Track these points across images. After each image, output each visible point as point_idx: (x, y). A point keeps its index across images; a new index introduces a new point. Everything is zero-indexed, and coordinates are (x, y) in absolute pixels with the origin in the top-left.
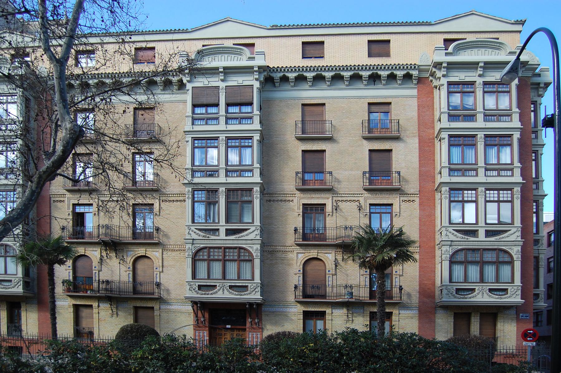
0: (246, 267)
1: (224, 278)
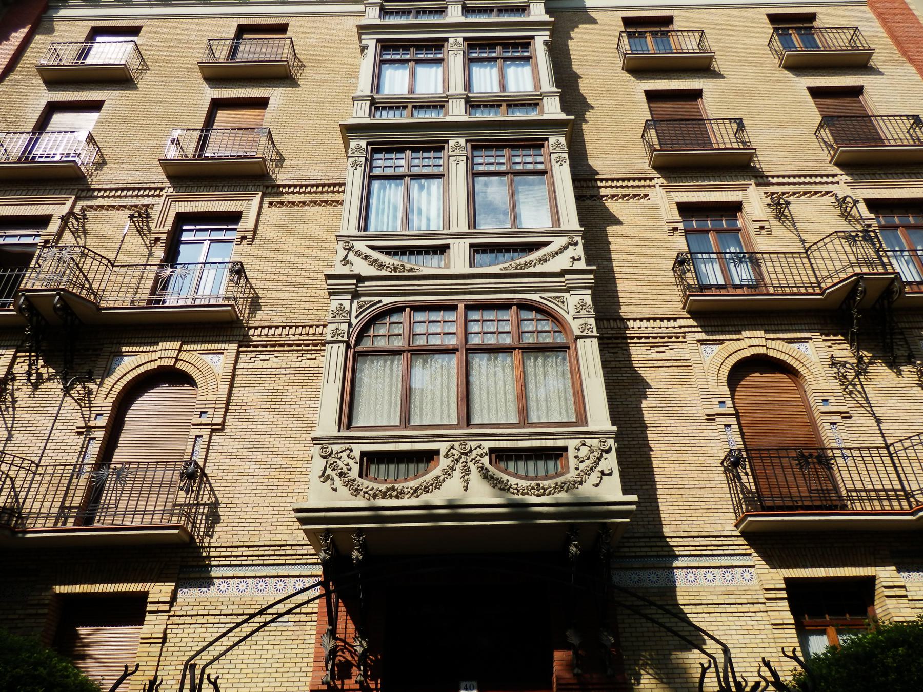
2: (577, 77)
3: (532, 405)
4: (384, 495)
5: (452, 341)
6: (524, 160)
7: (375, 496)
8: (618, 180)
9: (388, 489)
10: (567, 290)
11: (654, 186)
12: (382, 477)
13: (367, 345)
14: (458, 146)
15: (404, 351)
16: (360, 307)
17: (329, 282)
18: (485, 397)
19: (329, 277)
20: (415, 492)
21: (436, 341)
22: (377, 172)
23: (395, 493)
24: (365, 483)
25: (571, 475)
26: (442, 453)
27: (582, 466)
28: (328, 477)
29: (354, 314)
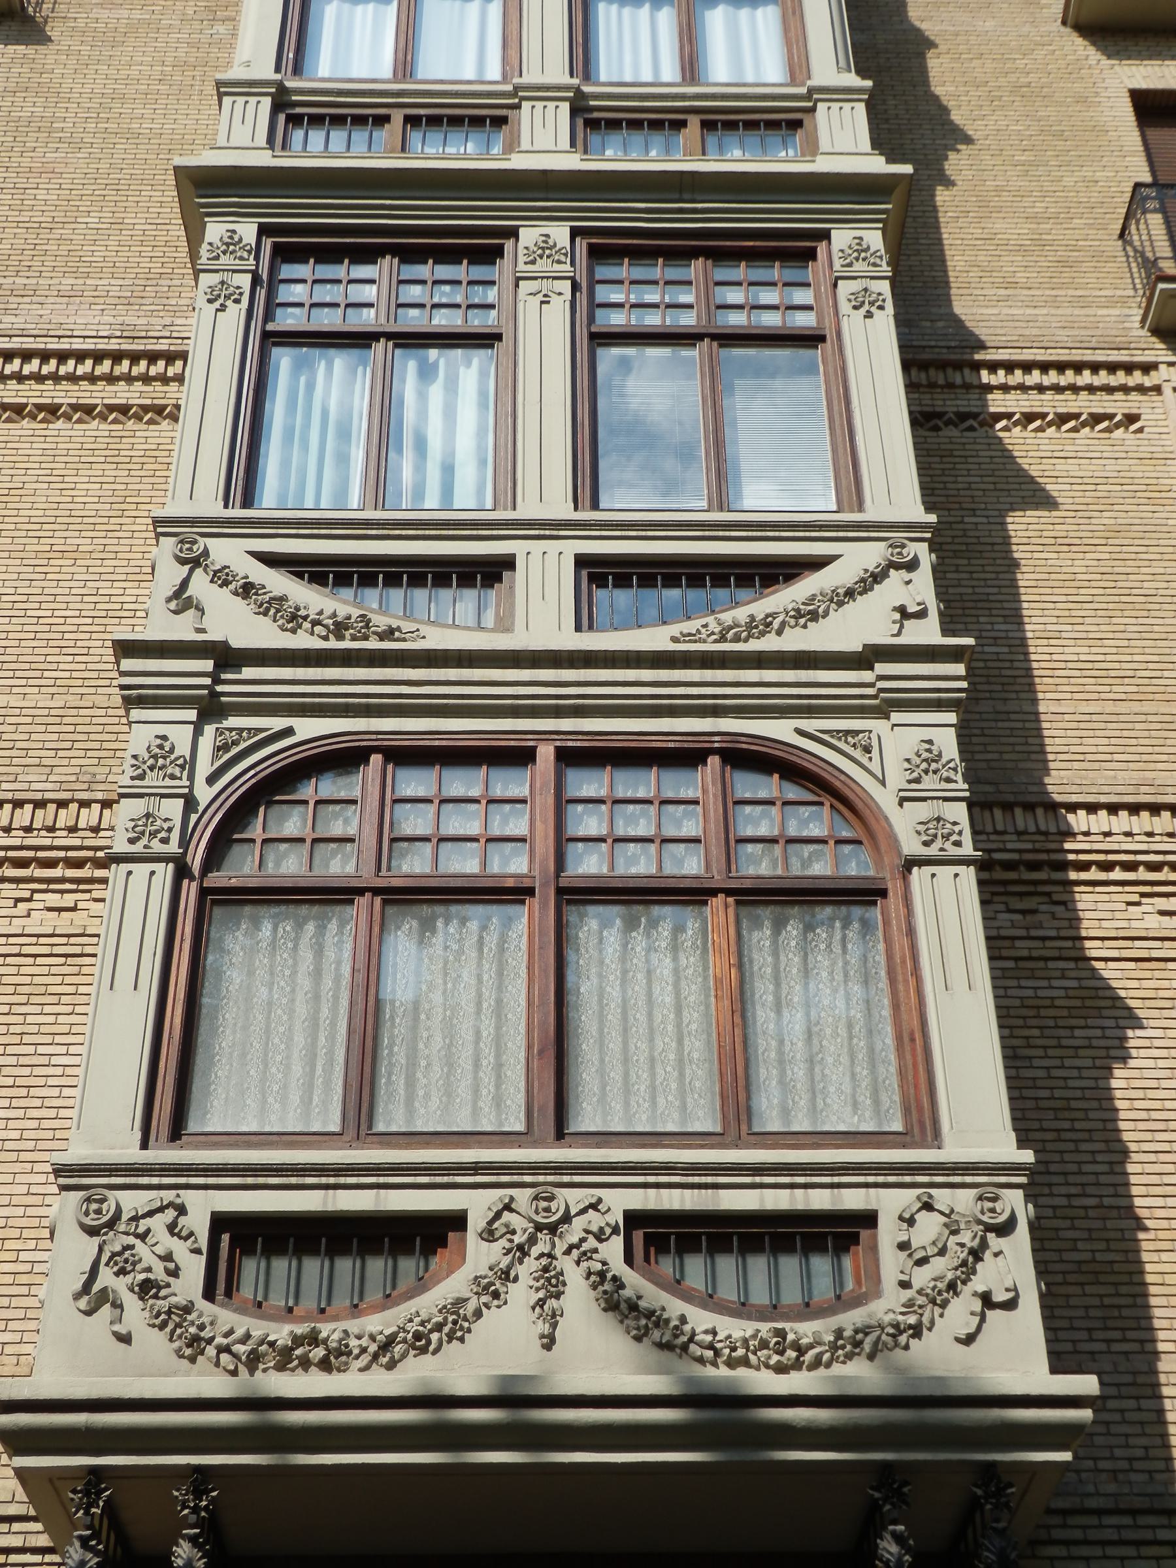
0: (815, 991)
1: (556, 1112)
2: (921, 44)
3: (766, 1075)
4: (285, 1359)
5: (514, 864)
6: (753, 297)
7: (253, 1361)
8: (1045, 367)
9: (298, 1341)
10: (882, 711)
11: (1157, 389)
12: (277, 1300)
13: (242, 868)
14: (546, 247)
15: (361, 891)
16: (225, 748)
17: (127, 664)
18: (614, 1045)
19: (126, 649)
20: (385, 1350)
21: (463, 864)
22: (288, 320)
23: (319, 1353)
24: (224, 1319)
25: (887, 1305)
26: (476, 1223)
27: (922, 1277)
28: (104, 1297)
29: (204, 767)
